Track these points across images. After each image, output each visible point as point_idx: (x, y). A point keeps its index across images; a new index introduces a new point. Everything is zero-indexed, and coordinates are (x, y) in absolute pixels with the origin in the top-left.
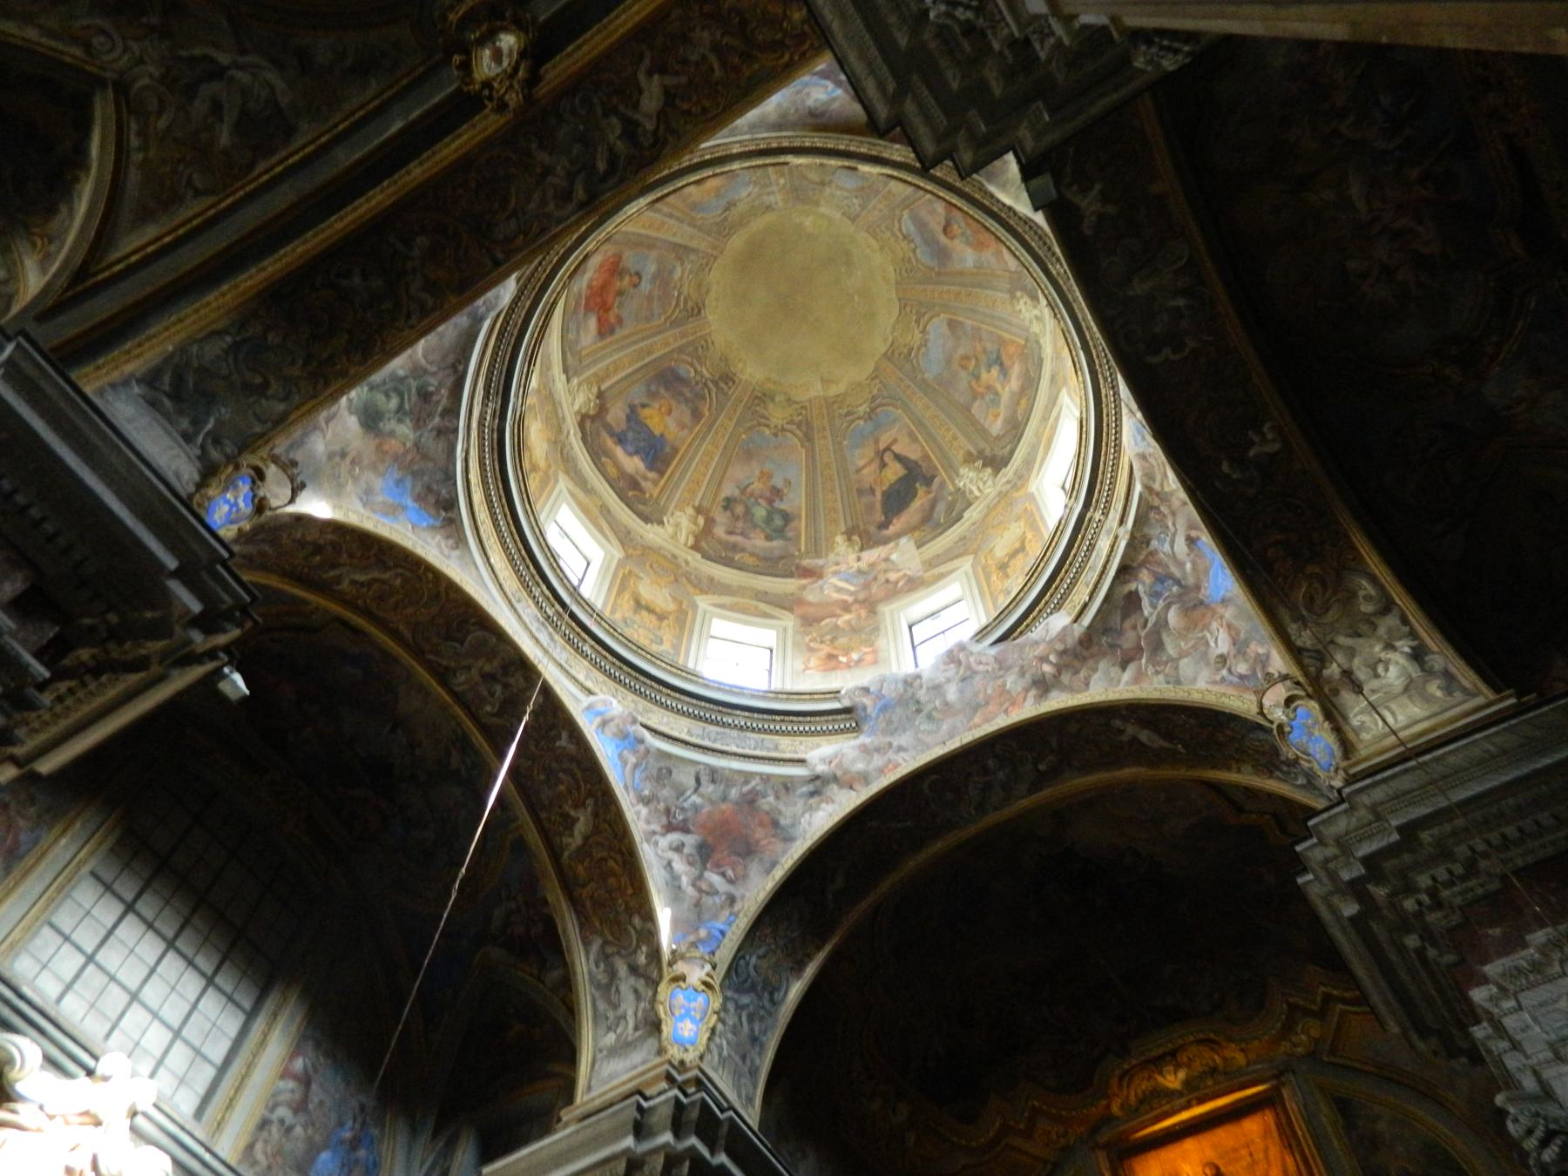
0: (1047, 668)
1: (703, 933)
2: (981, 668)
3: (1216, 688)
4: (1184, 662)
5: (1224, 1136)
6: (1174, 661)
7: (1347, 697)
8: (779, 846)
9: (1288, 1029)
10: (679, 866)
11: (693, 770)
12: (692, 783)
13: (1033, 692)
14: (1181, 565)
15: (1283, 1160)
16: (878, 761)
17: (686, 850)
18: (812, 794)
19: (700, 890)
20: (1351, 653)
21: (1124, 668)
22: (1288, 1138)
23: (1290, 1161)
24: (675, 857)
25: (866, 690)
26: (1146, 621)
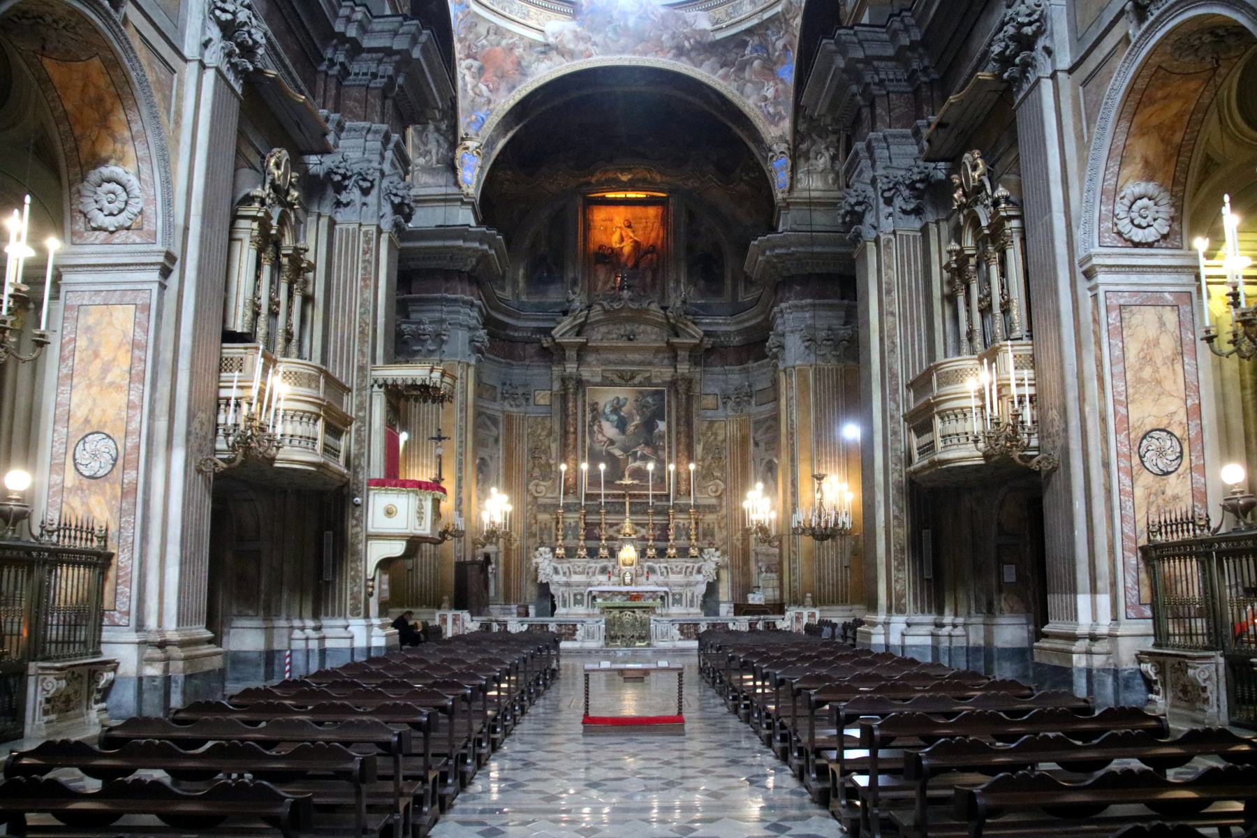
0: (686, 44)
1: (473, 117)
2: (652, 16)
3: (758, 112)
4: (749, 85)
5: (638, 210)
6: (747, 81)
7: (802, 161)
8: (518, 77)
10: (468, 78)
11: (487, 26)
12: (485, 33)
13: (674, 51)
14: (775, 50)
16: (582, 47)
17: (473, 70)
18: (542, 53)
19: (476, 94)
20: (814, 143)
21: (722, 67)
22: (664, 221)
23: (661, 231)
24: (466, 72)
26: (744, 55)
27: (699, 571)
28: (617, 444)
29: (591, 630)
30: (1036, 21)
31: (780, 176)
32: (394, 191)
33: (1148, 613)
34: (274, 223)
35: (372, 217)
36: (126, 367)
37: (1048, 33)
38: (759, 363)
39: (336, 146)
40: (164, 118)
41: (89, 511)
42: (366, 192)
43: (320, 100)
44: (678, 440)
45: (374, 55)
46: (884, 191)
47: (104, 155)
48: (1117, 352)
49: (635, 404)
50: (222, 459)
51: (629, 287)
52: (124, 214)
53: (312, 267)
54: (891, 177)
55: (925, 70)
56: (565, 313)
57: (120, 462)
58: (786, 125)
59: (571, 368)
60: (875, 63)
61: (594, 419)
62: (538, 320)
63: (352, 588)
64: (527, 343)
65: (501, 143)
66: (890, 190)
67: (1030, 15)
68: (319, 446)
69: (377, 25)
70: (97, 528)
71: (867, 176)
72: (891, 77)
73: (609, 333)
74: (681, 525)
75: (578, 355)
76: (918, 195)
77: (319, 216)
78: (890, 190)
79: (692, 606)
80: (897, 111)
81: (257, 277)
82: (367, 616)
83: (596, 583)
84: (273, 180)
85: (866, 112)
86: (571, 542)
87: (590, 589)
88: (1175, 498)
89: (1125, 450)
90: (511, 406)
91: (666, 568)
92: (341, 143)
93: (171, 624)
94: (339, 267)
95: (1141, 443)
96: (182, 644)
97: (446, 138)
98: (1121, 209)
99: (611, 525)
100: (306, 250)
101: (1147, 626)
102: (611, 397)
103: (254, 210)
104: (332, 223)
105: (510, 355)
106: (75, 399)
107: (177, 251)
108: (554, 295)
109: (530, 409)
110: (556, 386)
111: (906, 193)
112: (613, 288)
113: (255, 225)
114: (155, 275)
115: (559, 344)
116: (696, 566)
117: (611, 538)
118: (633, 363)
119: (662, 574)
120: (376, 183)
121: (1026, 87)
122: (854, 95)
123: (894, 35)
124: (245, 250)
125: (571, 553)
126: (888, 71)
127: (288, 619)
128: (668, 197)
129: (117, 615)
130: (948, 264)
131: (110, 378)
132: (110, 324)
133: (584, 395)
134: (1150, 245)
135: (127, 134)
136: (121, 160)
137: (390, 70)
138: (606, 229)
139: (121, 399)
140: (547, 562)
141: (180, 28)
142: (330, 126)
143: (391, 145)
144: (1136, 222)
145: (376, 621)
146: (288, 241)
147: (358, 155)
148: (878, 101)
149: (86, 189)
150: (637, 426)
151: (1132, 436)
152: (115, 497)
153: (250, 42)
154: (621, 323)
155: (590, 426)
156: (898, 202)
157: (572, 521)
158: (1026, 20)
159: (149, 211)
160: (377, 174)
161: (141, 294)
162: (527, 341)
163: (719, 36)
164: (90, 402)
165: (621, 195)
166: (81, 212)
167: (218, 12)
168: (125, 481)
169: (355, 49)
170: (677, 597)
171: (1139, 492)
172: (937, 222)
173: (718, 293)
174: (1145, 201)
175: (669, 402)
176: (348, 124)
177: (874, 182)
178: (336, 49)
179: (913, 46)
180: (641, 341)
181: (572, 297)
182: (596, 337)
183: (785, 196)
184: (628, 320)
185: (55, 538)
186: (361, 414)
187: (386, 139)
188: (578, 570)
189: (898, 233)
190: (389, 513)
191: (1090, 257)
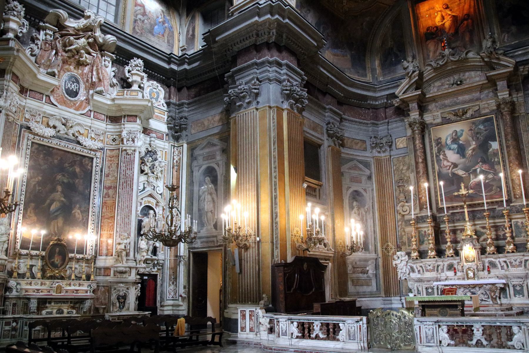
15: (470, 3)
28: (459, 167)
29: (352, 331)
49: (470, 133)
61: (439, 150)
62: (389, 89)
64: (386, 108)
73: (442, 85)
74: (519, 224)
86: (423, 247)
90: (379, 152)
91: (505, 262)
102: (450, 132)
109: (392, 153)
110: (409, 132)
119: (502, 267)
125: (422, 255)
133: (430, 134)
138: (430, 16)
140: (404, 263)
150: (474, 150)
155: (437, 156)
170: (518, 288)
175: (498, 125)
188: (429, 268)
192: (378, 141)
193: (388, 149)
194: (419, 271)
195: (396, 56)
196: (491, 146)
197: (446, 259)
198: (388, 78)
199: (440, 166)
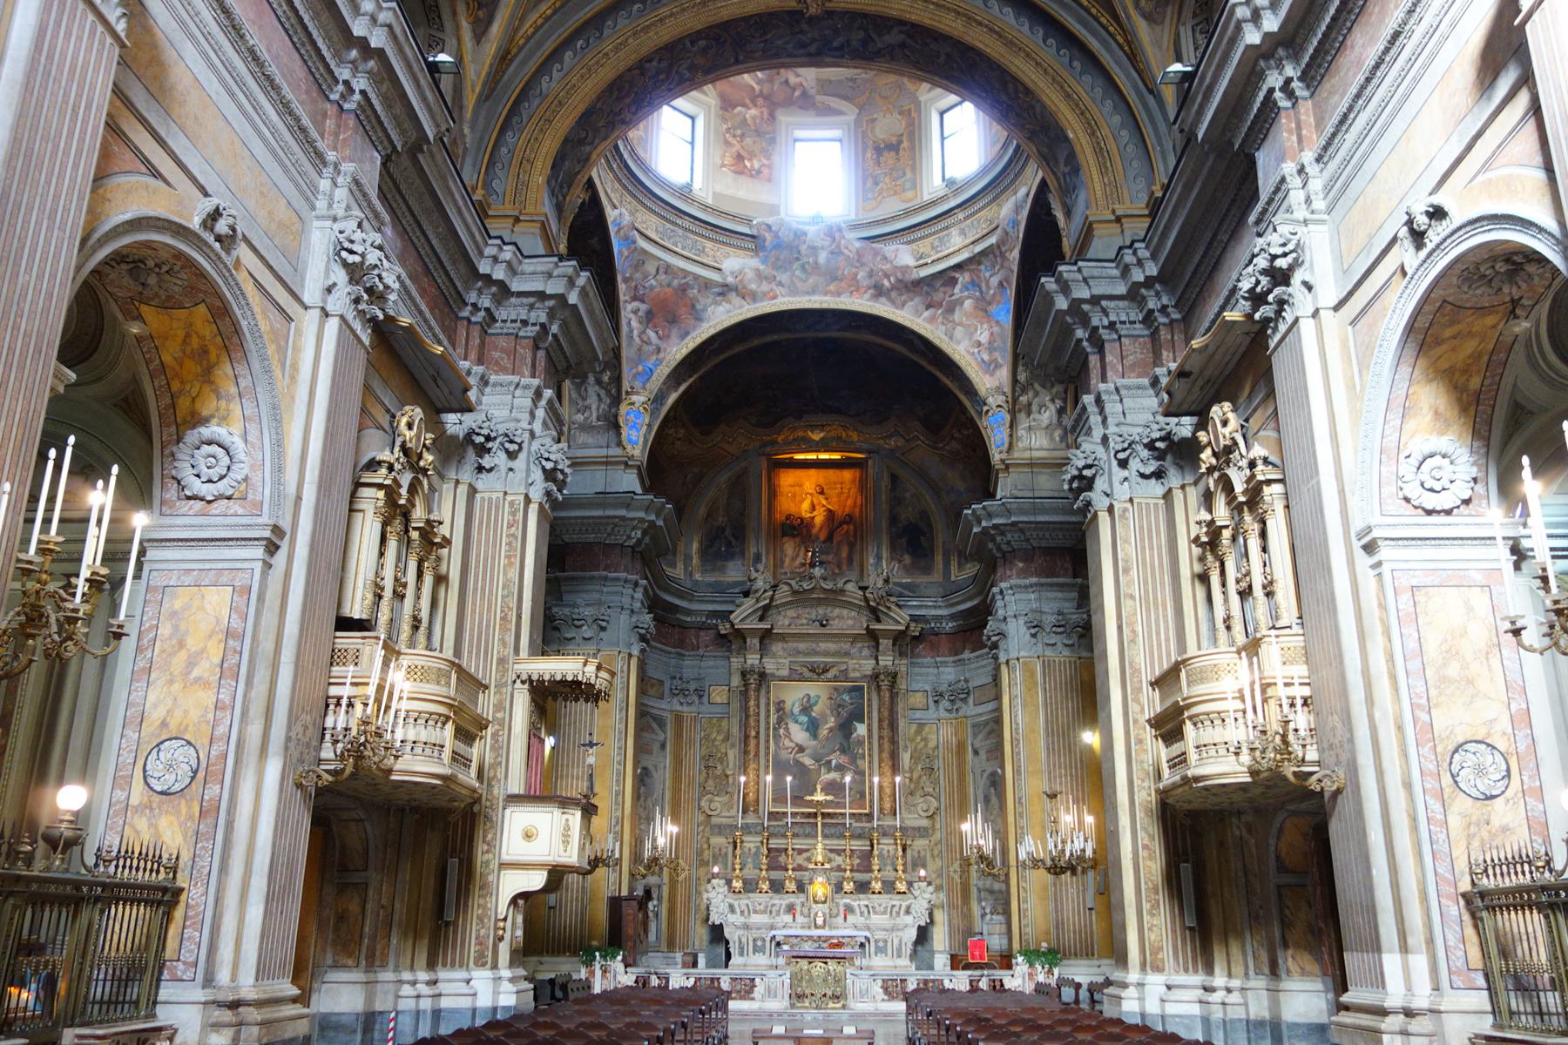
0: (886, 283)
1: (640, 368)
2: (846, 251)
3: (968, 358)
4: (959, 328)
5: (831, 474)
7: (1022, 416)
9: (890, 436)
10: (634, 324)
11: (656, 264)
13: (871, 291)
14: (988, 287)
16: (765, 287)
17: (640, 314)
18: (720, 294)
20: (1037, 394)
22: (862, 485)
24: (632, 316)
25: (769, 227)
27: (908, 912)
28: (807, 752)
29: (773, 987)
30: (1291, 252)
31: (996, 435)
32: (546, 455)
33: (1481, 982)
34: (404, 491)
35: (520, 485)
36: (217, 660)
37: (1307, 264)
38: (978, 653)
39: (479, 402)
40: (278, 373)
41: (158, 835)
42: (512, 456)
43: (460, 350)
44: (880, 746)
45: (525, 300)
46: (1117, 452)
47: (205, 413)
48: (1412, 645)
50: (327, 771)
51: (821, 563)
52: (225, 480)
53: (447, 542)
54: (1126, 435)
55: (1163, 309)
56: (746, 594)
57: (201, 774)
58: (1004, 374)
59: (753, 659)
60: (1104, 303)
61: (780, 721)
62: (714, 602)
63: (478, 931)
65: (673, 398)
66: (1124, 450)
67: (1284, 245)
68: (446, 755)
69: (528, 266)
70: (165, 856)
71: (1098, 433)
72: (1123, 318)
73: (798, 617)
75: (761, 643)
76: (1161, 455)
77: (457, 482)
78: (1124, 450)
79: (899, 956)
80: (1131, 358)
81: (381, 554)
82: (495, 967)
83: (780, 925)
84: (404, 442)
85: (1094, 360)
86: (750, 872)
87: (773, 933)
88: (1505, 829)
89: (1432, 767)
90: (682, 704)
92: (485, 399)
93: (247, 978)
94: (479, 541)
95: (1452, 758)
96: (259, 1004)
97: (608, 392)
98: (1407, 469)
99: (800, 852)
100: (441, 523)
101: (1481, 1000)
103: (381, 476)
104: (473, 491)
105: (681, 644)
106: (152, 697)
107: (286, 525)
108: (734, 572)
109: (703, 708)
110: (736, 681)
111: (1145, 453)
112: (803, 565)
113: (381, 494)
114: (259, 552)
115: (738, 630)
116: (904, 905)
117: (799, 868)
118: (827, 654)
119: (862, 914)
120: (525, 445)
121: (1283, 328)
122: (1080, 341)
123: (1126, 271)
124: (368, 523)
125: (750, 886)
126: (1120, 312)
127: (397, 969)
128: (866, 460)
129: (181, 966)
130: (1197, 538)
131: (195, 673)
132: (201, 608)
133: (769, 692)
134: (1448, 512)
135: (233, 390)
136: (224, 420)
137: (543, 318)
138: (794, 496)
139: (208, 698)
141: (298, 269)
142: (472, 380)
143: (543, 403)
144: (1427, 486)
145: (506, 973)
146: (419, 514)
147: (506, 413)
148: (1107, 345)
149: (183, 452)
150: (831, 730)
151: (1439, 749)
152: (191, 817)
153: (381, 287)
154: (812, 606)
155: (774, 729)
156: (1135, 464)
157: (752, 845)
158: (1279, 251)
159: (256, 478)
160: (527, 435)
161: (240, 574)
162: (702, 627)
163: (924, 273)
164: (169, 701)
165: (812, 456)
166: (173, 478)
167: (344, 254)
168: (206, 797)
169: (503, 292)
170: (881, 944)
171: (1454, 821)
172: (1183, 487)
173: (927, 570)
174: (1437, 460)
176: (493, 378)
177: (1105, 439)
178: (480, 292)
179: (1149, 282)
180: (836, 626)
181: (754, 575)
182: (783, 621)
183: (1004, 456)
184: (819, 602)
185: (112, 869)
186: (499, 715)
187: (538, 394)
188: (758, 908)
189: (1135, 501)
190: (528, 836)
191: (1369, 529)
192: (684, 685)
193: (696, 699)
194: (742, 912)
195: (729, 544)
196: (856, 730)
197: (786, 896)
198: (711, 578)
199: (777, 744)
